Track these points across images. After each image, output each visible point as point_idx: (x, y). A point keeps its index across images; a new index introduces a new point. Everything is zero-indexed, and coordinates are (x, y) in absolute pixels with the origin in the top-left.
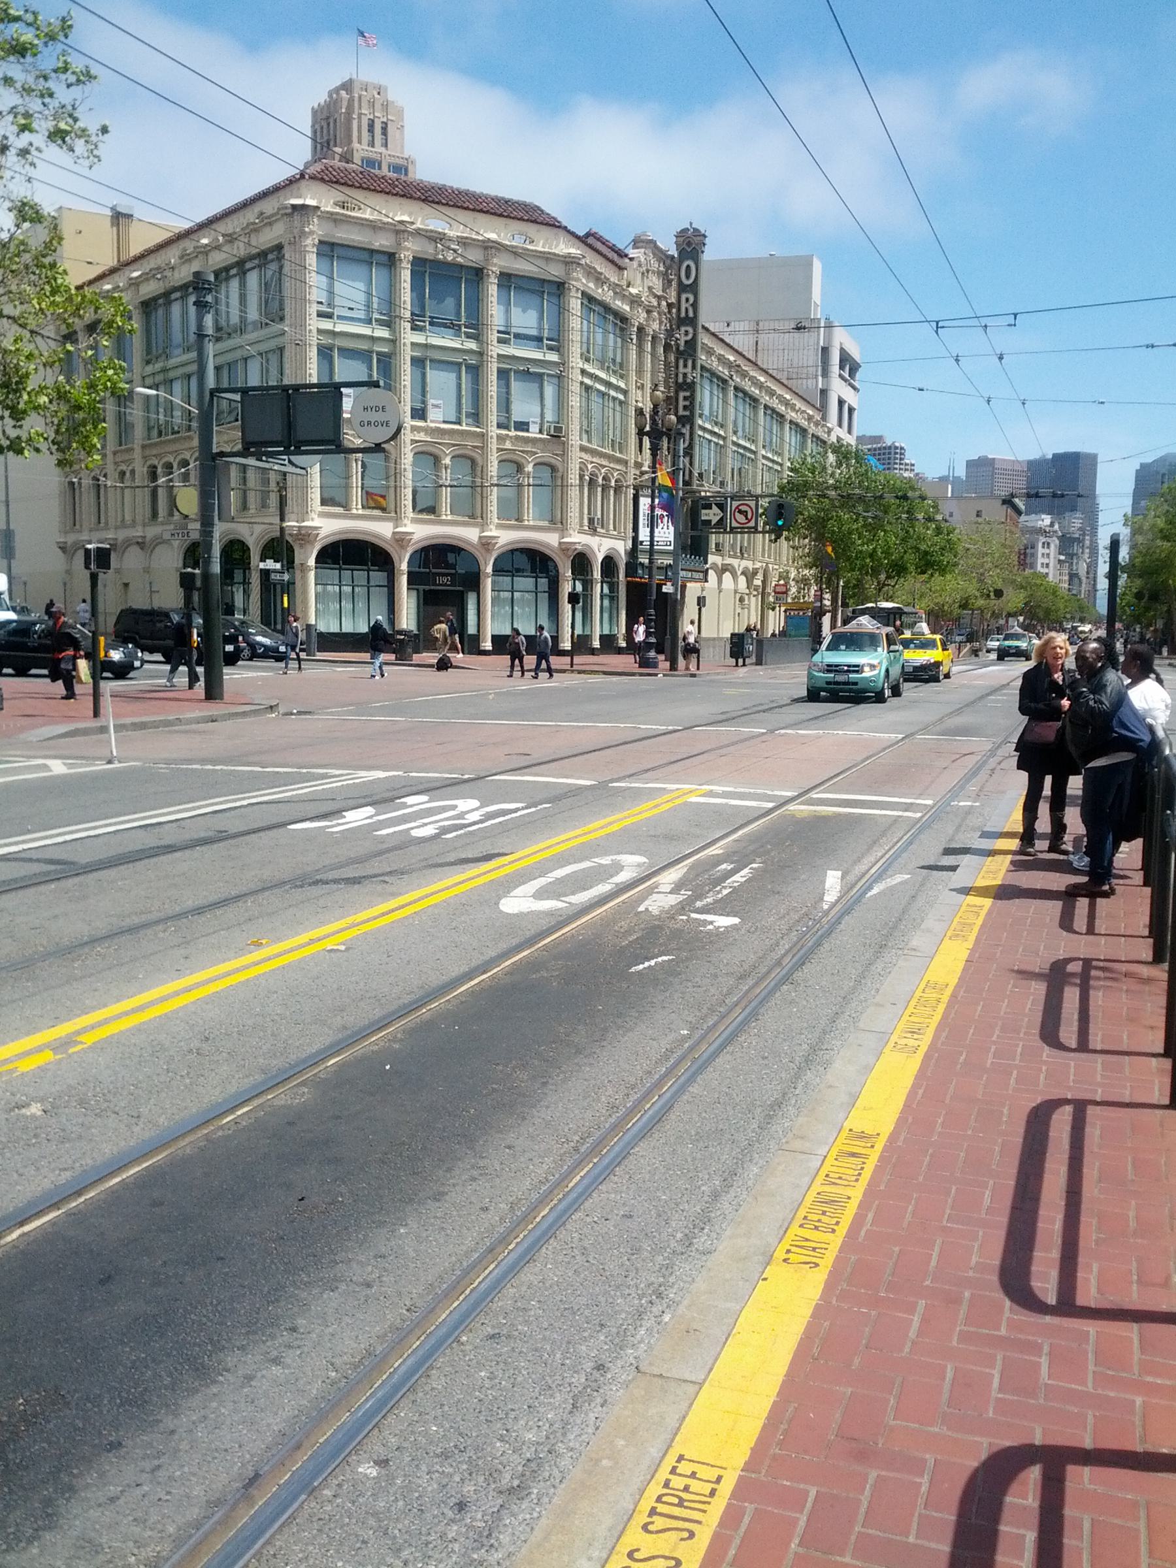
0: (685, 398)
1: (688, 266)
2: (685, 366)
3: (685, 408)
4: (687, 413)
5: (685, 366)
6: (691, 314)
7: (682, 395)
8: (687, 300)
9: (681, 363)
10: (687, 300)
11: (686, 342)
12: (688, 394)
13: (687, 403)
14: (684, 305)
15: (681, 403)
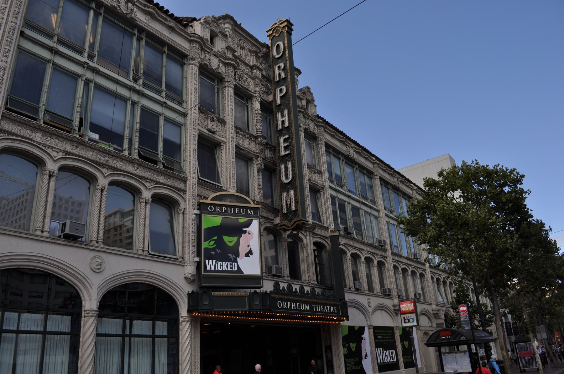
0: (285, 140)
1: (278, 45)
2: (283, 116)
3: (286, 148)
4: (288, 152)
5: (283, 116)
6: (283, 76)
7: (282, 140)
8: (279, 67)
9: (279, 114)
10: (279, 67)
11: (281, 97)
12: (287, 136)
13: (287, 144)
14: (277, 72)
15: (282, 145)
